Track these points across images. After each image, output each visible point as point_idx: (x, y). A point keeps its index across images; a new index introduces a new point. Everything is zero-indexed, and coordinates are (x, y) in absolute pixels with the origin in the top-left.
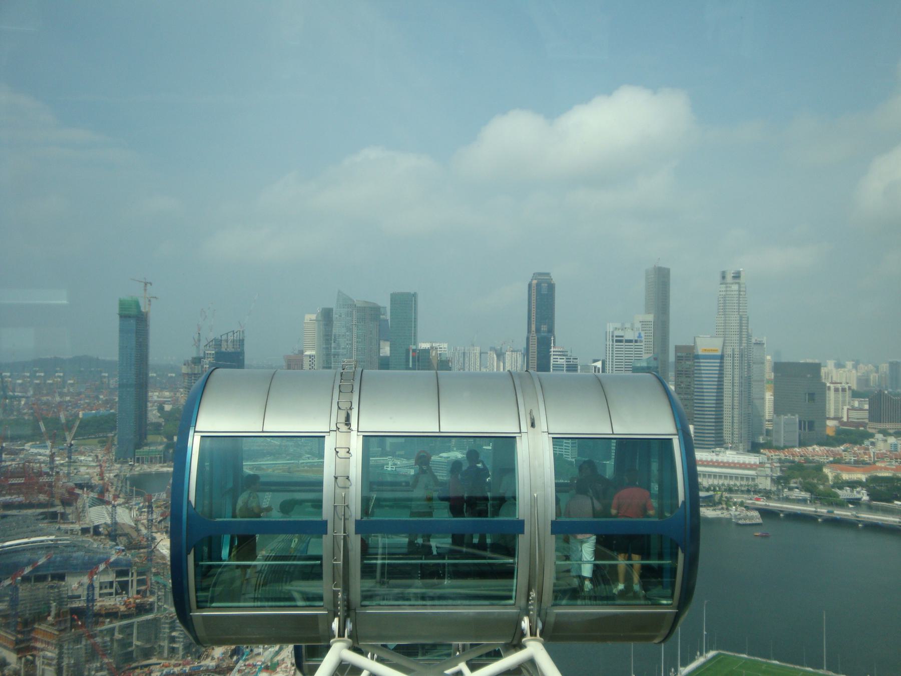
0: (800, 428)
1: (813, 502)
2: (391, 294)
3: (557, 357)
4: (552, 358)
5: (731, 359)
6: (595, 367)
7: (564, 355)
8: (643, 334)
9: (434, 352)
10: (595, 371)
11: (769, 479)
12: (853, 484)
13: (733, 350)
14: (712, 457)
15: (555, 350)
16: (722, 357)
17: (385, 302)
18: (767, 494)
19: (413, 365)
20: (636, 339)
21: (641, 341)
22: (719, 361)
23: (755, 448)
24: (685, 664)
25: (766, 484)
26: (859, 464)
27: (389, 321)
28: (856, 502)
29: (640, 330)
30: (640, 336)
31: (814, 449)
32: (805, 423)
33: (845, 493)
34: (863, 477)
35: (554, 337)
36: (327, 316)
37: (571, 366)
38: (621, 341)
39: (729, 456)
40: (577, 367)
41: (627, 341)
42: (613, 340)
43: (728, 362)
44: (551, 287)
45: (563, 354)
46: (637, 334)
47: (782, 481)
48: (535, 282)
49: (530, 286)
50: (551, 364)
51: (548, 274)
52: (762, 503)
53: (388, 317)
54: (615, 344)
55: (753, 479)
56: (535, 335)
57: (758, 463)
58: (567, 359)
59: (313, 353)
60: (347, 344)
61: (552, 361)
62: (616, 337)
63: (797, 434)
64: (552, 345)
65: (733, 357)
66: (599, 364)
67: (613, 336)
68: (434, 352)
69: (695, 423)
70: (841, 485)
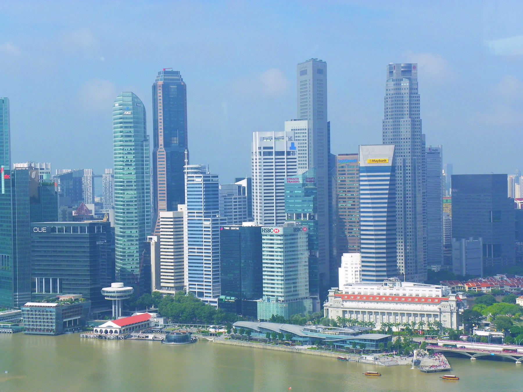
0: (485, 255)
3: (193, 175)
4: (186, 177)
5: (402, 172)
6: (240, 187)
7: (201, 173)
8: (296, 145)
9: (34, 174)
10: (239, 191)
11: (455, 315)
13: (404, 160)
14: (385, 291)
15: (189, 166)
16: (393, 169)
19: (6, 191)
20: (289, 150)
21: (294, 154)
22: (389, 174)
29: (293, 139)
30: (293, 147)
31: (502, 278)
32: (490, 246)
35: (188, 151)
37: (210, 186)
38: (270, 154)
40: (218, 187)
41: (278, 153)
42: (260, 152)
43: (399, 174)
44: (182, 89)
45: (200, 171)
46: (290, 145)
48: (161, 83)
49: (155, 87)
50: (186, 184)
51: (177, 73)
54: (262, 157)
55: (435, 316)
56: (163, 150)
57: (440, 296)
58: (204, 177)
61: (186, 180)
62: (264, 148)
63: (482, 260)
64: (186, 160)
65: (404, 170)
66: (244, 183)
67: (260, 148)
68: (34, 174)
69: (363, 250)
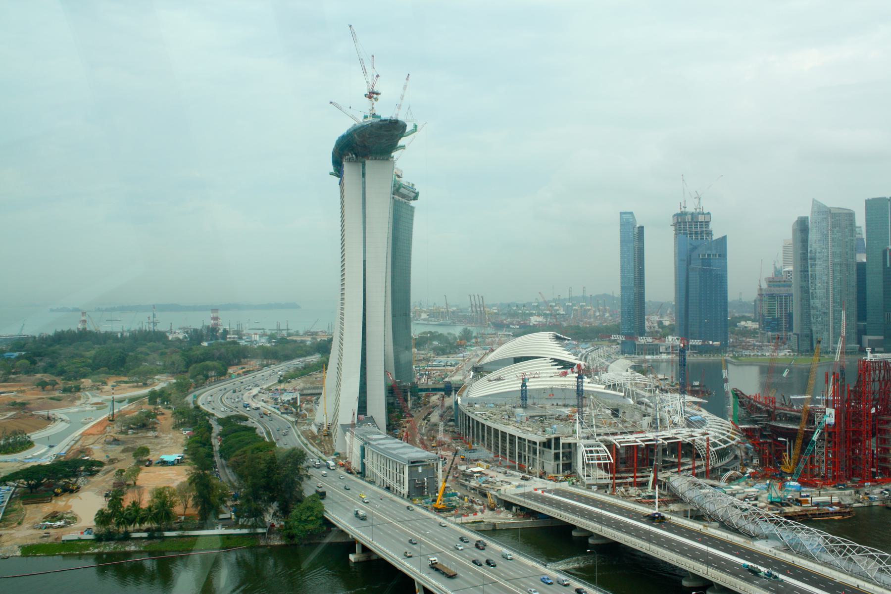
2: (866, 201)
17: (860, 220)
27: (865, 240)
36: (802, 227)
53: (864, 236)
59: (791, 268)
60: (823, 248)
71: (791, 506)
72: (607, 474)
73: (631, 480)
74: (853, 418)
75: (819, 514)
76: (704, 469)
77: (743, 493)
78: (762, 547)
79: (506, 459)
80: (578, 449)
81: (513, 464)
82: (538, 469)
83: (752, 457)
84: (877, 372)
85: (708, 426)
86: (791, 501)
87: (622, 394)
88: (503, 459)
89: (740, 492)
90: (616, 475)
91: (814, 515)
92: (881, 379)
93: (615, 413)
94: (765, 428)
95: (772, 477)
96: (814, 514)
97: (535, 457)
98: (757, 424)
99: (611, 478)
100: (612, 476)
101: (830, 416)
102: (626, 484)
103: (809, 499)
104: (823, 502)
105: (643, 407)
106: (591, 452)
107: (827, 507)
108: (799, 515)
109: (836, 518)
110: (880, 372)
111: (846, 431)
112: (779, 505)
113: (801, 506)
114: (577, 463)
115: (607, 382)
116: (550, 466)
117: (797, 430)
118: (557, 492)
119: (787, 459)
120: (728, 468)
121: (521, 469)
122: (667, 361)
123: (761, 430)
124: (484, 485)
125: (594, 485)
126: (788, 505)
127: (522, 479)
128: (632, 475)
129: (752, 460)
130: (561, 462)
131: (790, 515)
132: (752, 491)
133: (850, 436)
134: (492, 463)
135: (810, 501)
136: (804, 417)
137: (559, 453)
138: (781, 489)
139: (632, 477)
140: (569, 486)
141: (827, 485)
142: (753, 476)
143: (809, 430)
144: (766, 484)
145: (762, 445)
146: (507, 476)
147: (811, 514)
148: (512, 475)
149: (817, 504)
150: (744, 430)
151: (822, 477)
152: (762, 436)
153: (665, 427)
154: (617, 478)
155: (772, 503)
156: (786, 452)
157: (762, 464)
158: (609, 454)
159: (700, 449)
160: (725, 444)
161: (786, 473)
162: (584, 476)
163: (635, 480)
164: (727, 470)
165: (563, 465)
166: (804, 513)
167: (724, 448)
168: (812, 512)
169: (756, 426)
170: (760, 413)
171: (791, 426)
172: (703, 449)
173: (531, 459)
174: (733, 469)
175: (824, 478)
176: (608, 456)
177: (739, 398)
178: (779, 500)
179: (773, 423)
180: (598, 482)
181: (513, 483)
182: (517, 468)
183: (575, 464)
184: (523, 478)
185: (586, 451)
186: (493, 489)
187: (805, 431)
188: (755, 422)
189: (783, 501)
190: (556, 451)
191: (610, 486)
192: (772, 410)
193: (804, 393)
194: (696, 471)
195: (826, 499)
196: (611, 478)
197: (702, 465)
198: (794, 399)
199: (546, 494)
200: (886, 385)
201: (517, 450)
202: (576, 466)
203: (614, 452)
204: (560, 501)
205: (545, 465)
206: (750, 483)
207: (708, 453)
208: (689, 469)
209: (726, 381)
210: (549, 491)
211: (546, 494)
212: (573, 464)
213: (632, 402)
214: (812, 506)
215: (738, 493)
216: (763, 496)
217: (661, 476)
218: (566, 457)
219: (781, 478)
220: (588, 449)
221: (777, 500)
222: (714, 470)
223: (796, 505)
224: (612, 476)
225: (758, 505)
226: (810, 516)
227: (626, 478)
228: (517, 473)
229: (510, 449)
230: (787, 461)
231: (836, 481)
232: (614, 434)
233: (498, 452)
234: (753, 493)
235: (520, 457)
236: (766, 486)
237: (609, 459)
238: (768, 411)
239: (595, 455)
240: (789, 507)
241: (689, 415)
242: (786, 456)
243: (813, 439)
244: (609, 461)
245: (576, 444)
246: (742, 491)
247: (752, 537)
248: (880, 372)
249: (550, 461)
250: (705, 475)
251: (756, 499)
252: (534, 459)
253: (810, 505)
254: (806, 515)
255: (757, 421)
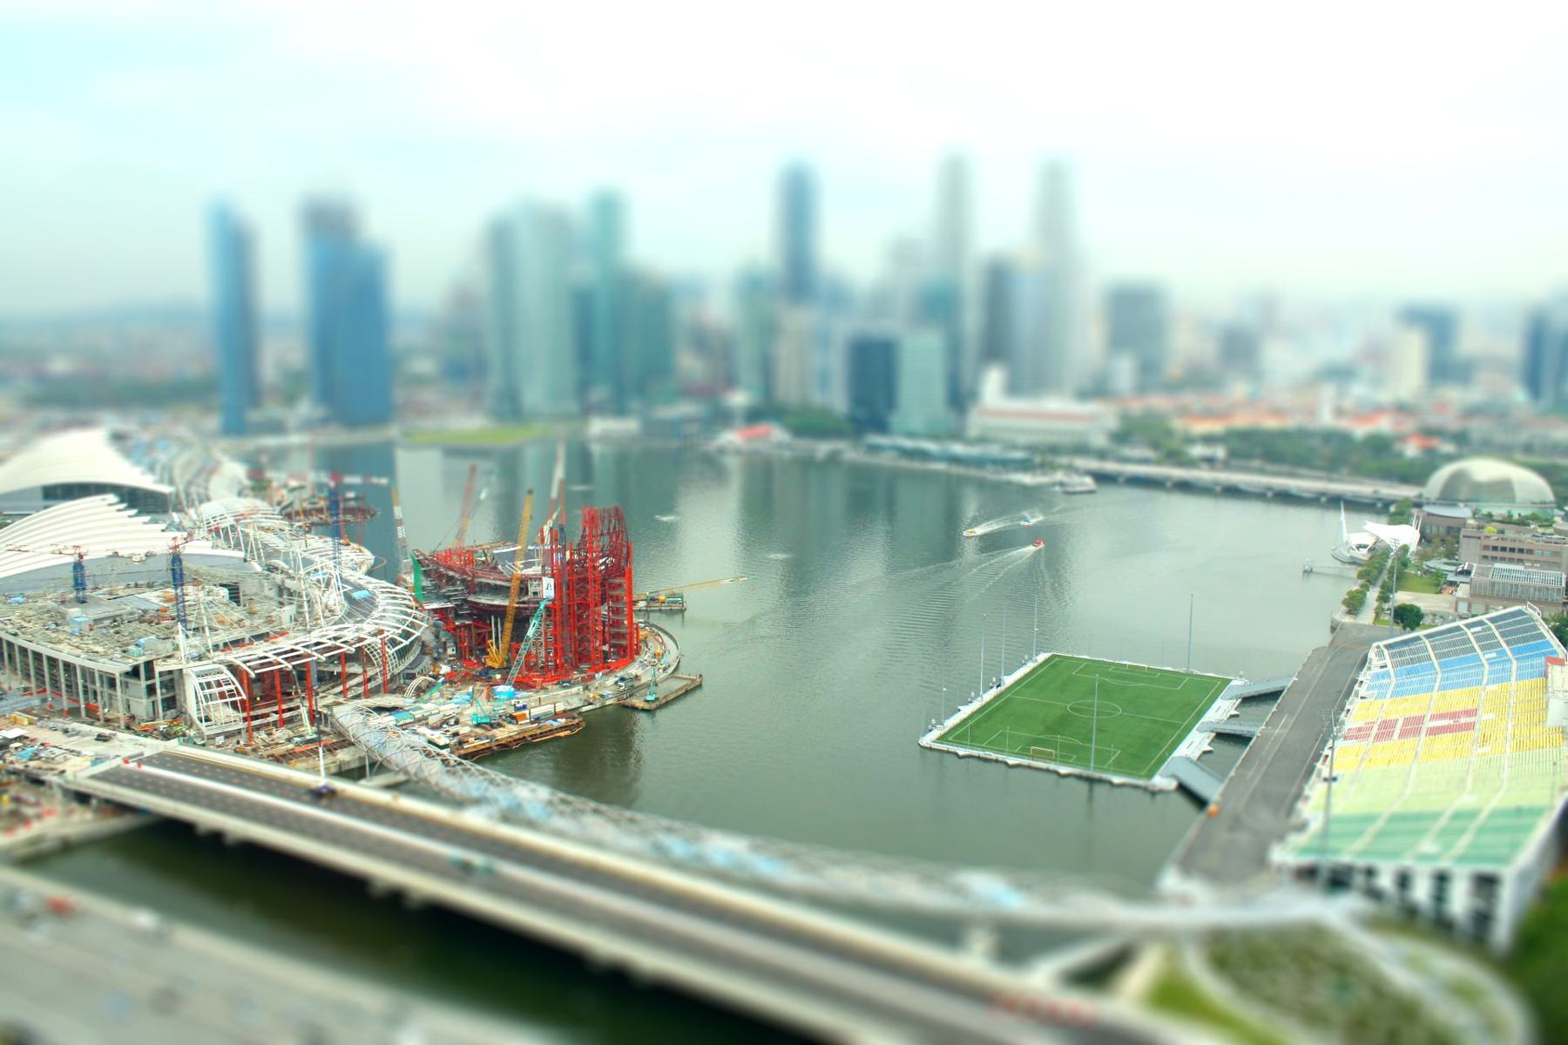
1: (1158, 463)
12: (1209, 439)
18: (1102, 455)
23: (1083, 395)
24: (1009, 672)
25: (1099, 441)
26: (1209, 414)
28: (1210, 461)
33: (1198, 451)
34: (1216, 427)
39: (1054, 404)
47: (1122, 436)
52: (1094, 464)
70: (1190, 440)
71: (504, 727)
72: (236, 714)
73: (275, 717)
74: (578, 586)
75: (541, 733)
76: (380, 680)
77: (438, 713)
78: (473, 819)
79: (61, 696)
80: (186, 677)
81: (74, 705)
82: (121, 714)
83: (445, 643)
84: (606, 521)
85: (380, 608)
86: (504, 718)
87: (241, 554)
88: (55, 696)
89: (433, 712)
90: (252, 713)
91: (534, 736)
92: (612, 531)
93: (235, 594)
94: (462, 605)
95: (475, 679)
96: (536, 735)
97: (111, 692)
98: (450, 601)
99: (245, 719)
100: (245, 715)
101: (547, 589)
102: (268, 724)
103: (527, 712)
104: (546, 714)
105: (278, 577)
106: (209, 685)
107: (551, 722)
108: (515, 741)
109: (562, 734)
110: (610, 521)
111: (569, 606)
112: (489, 728)
113: (517, 723)
114: (185, 696)
115: (212, 521)
116: (141, 706)
117: (505, 607)
118: (163, 760)
119: (494, 648)
120: (412, 671)
121: (92, 715)
122: (301, 448)
123: (455, 609)
124: (33, 764)
125: (218, 735)
126: (500, 725)
127: (97, 740)
128: (276, 708)
129: (445, 649)
130: (159, 697)
131: (503, 742)
132: (449, 709)
133: (574, 611)
134: (42, 715)
135: (528, 715)
136: (515, 585)
137: (154, 684)
138: (489, 697)
139: (276, 712)
140: (180, 744)
141: (548, 681)
142: (450, 679)
143: (522, 605)
144: (468, 694)
145: (458, 630)
146: (69, 736)
147: (530, 736)
148: (78, 733)
149: (537, 719)
150: (435, 611)
151: (542, 668)
152: (458, 616)
153: (317, 619)
154: (256, 718)
155: (478, 725)
156: (491, 638)
157: (460, 655)
158: (238, 685)
159: (372, 652)
160: (407, 640)
161: (494, 668)
162: (201, 721)
163: (281, 716)
164: (412, 677)
165: (163, 700)
166: (521, 736)
167: (407, 645)
168: (531, 733)
169: (449, 605)
170: (454, 585)
171: (497, 602)
172: (376, 650)
173: (106, 695)
174: (421, 673)
175: (545, 668)
176: (236, 688)
177: (423, 566)
178: (488, 721)
179: (472, 598)
180: (226, 730)
181: (84, 753)
182: (83, 713)
183: (183, 699)
184: (101, 738)
185: (201, 684)
186: (52, 769)
187: (517, 608)
188: (448, 598)
189: (493, 721)
190: (149, 682)
191: (243, 732)
192: (469, 579)
193: (515, 542)
194: (370, 685)
195: (548, 708)
196: (245, 719)
197: (377, 674)
198: (498, 554)
199: (146, 769)
200: (618, 537)
201: (80, 682)
202: (185, 701)
203: (245, 682)
204: (173, 781)
205: (131, 703)
206: (447, 694)
207: (384, 655)
208: (358, 685)
209: (400, 522)
210: (150, 761)
211: (146, 769)
212: (177, 697)
213: (259, 569)
214: (532, 723)
215: (431, 715)
216: (466, 713)
217: (321, 703)
218: (166, 689)
219: (485, 676)
220: (203, 680)
221: (484, 721)
222: (393, 678)
223: (510, 723)
224: (245, 715)
225: (461, 732)
226: (530, 739)
227: (267, 715)
228: (86, 728)
229: (66, 680)
230: (494, 651)
231: (558, 673)
232: (237, 643)
233: (44, 683)
234: (451, 712)
235: (86, 692)
236: (468, 697)
237: (239, 694)
238: (464, 581)
239: (216, 690)
240: (501, 729)
241: (350, 588)
242: (492, 644)
243: (528, 634)
244: (240, 698)
245: (181, 670)
246: (437, 711)
247: (459, 803)
248: (610, 521)
249: (141, 698)
250: (382, 689)
251: (457, 722)
252: (110, 695)
253: (528, 721)
254: (524, 738)
255: (450, 596)
